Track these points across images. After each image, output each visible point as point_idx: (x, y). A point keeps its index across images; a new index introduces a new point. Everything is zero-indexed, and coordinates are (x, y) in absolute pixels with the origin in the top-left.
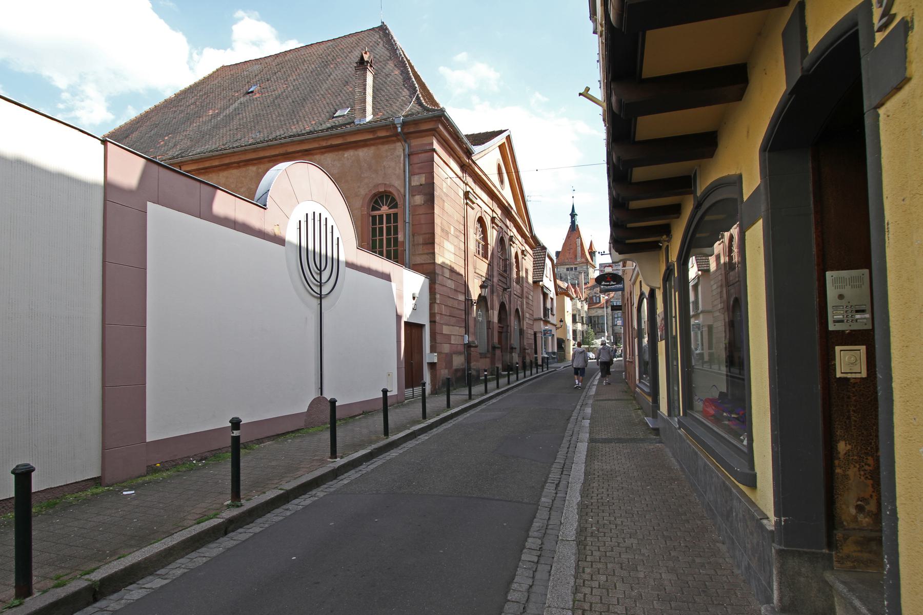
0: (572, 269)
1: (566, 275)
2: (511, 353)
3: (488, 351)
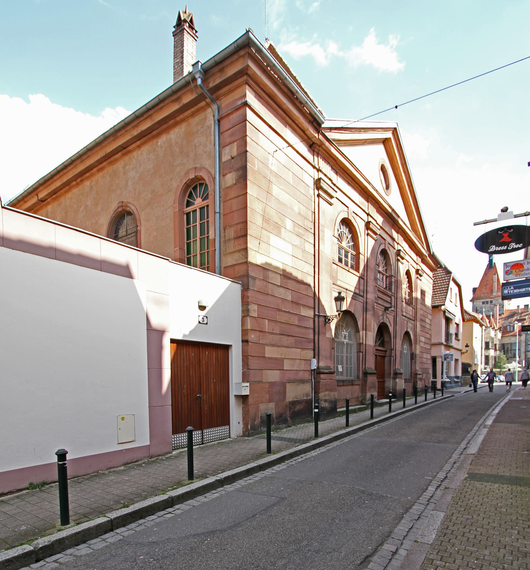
1: (482, 308)
2: (395, 378)
3: (358, 377)
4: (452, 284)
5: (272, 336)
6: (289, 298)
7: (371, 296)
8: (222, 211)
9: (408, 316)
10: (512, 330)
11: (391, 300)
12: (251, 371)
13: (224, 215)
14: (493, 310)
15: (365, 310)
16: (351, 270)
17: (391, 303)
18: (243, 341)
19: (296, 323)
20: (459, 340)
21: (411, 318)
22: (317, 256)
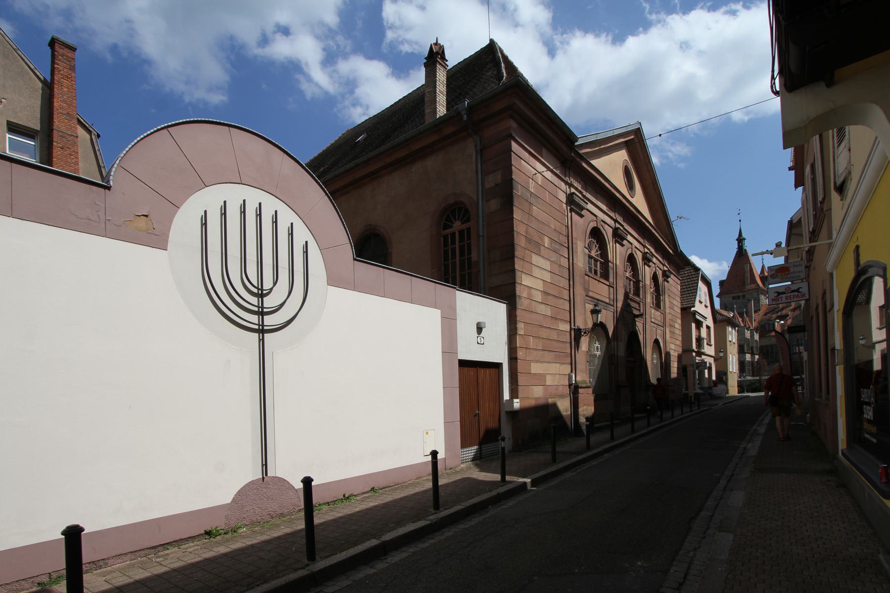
0: (739, 297)
4: (701, 284)
5: (536, 352)
6: (549, 314)
16: (602, 280)
19: (555, 337)
22: (571, 270)
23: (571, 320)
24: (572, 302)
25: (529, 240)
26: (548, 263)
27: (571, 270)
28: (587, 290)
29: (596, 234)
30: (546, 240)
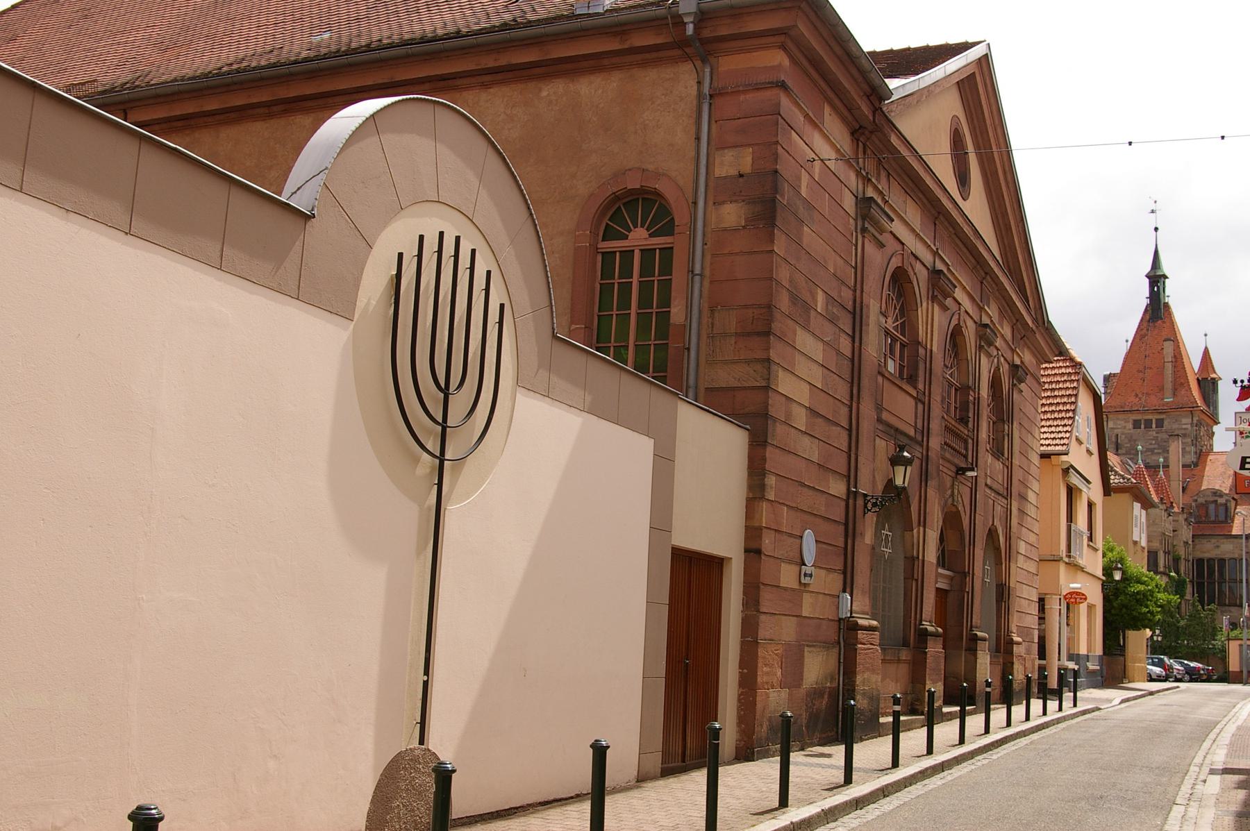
0: (1148, 424)
1: (1133, 440)
7: (935, 443)
8: (707, 272)
9: (995, 486)
10: (1222, 518)
11: (966, 449)
12: (763, 617)
13: (711, 282)
14: (1166, 451)
15: (924, 476)
17: (966, 457)
18: (747, 551)
20: (1096, 550)
21: (1001, 490)
23: (850, 476)
24: (853, 432)
25: (794, 298)
26: (820, 346)
27: (856, 361)
28: (879, 408)
29: (900, 280)
30: (820, 297)
